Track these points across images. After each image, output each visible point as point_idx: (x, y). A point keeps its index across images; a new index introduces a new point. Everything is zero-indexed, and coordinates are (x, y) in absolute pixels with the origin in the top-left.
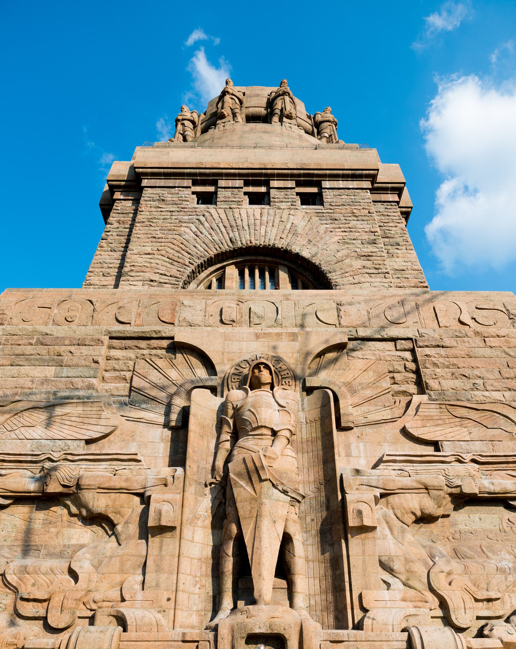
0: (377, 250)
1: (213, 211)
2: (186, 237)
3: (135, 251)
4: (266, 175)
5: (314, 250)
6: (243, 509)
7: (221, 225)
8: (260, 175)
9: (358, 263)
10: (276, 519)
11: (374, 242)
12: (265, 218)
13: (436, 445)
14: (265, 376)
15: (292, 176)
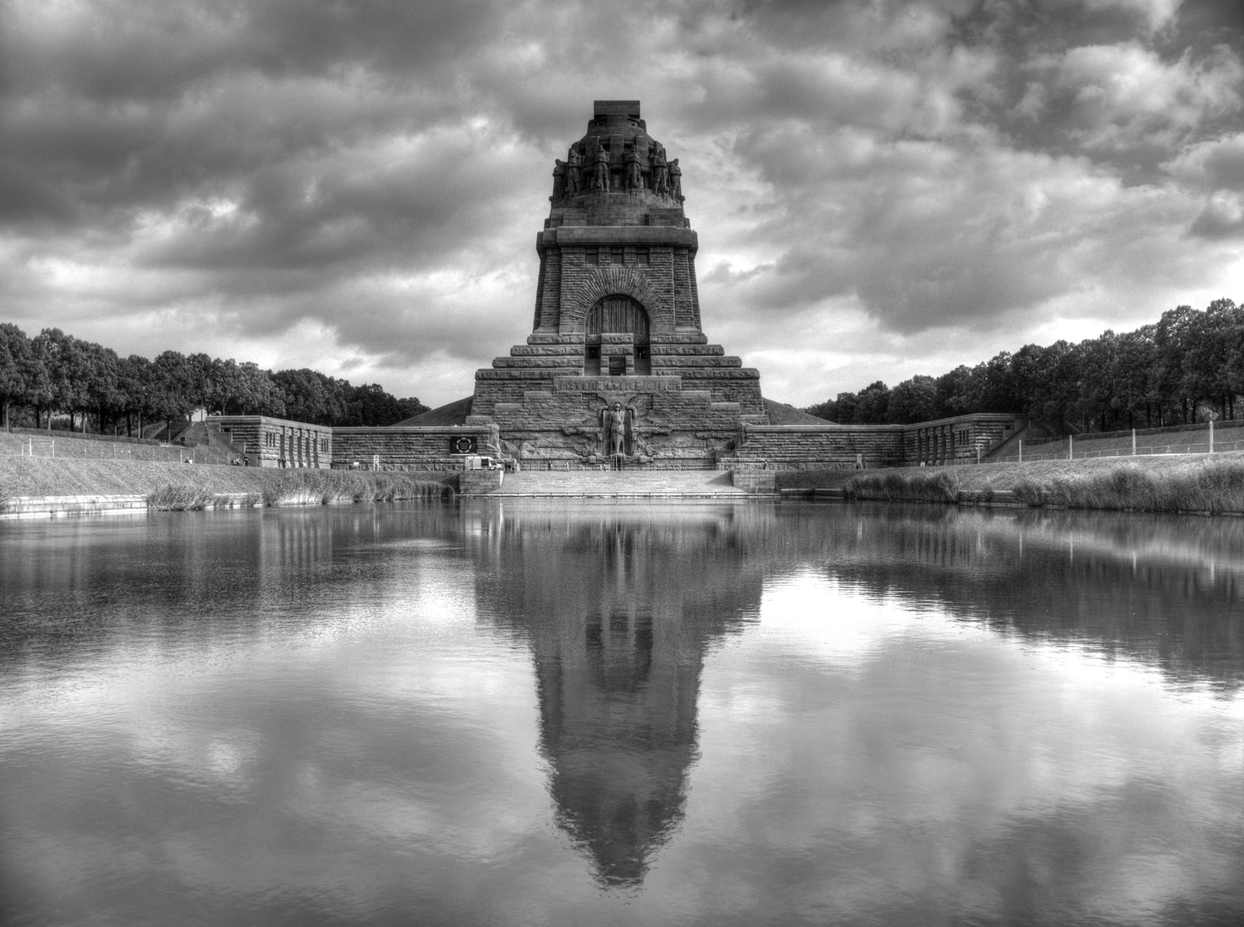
11: (669, 291)
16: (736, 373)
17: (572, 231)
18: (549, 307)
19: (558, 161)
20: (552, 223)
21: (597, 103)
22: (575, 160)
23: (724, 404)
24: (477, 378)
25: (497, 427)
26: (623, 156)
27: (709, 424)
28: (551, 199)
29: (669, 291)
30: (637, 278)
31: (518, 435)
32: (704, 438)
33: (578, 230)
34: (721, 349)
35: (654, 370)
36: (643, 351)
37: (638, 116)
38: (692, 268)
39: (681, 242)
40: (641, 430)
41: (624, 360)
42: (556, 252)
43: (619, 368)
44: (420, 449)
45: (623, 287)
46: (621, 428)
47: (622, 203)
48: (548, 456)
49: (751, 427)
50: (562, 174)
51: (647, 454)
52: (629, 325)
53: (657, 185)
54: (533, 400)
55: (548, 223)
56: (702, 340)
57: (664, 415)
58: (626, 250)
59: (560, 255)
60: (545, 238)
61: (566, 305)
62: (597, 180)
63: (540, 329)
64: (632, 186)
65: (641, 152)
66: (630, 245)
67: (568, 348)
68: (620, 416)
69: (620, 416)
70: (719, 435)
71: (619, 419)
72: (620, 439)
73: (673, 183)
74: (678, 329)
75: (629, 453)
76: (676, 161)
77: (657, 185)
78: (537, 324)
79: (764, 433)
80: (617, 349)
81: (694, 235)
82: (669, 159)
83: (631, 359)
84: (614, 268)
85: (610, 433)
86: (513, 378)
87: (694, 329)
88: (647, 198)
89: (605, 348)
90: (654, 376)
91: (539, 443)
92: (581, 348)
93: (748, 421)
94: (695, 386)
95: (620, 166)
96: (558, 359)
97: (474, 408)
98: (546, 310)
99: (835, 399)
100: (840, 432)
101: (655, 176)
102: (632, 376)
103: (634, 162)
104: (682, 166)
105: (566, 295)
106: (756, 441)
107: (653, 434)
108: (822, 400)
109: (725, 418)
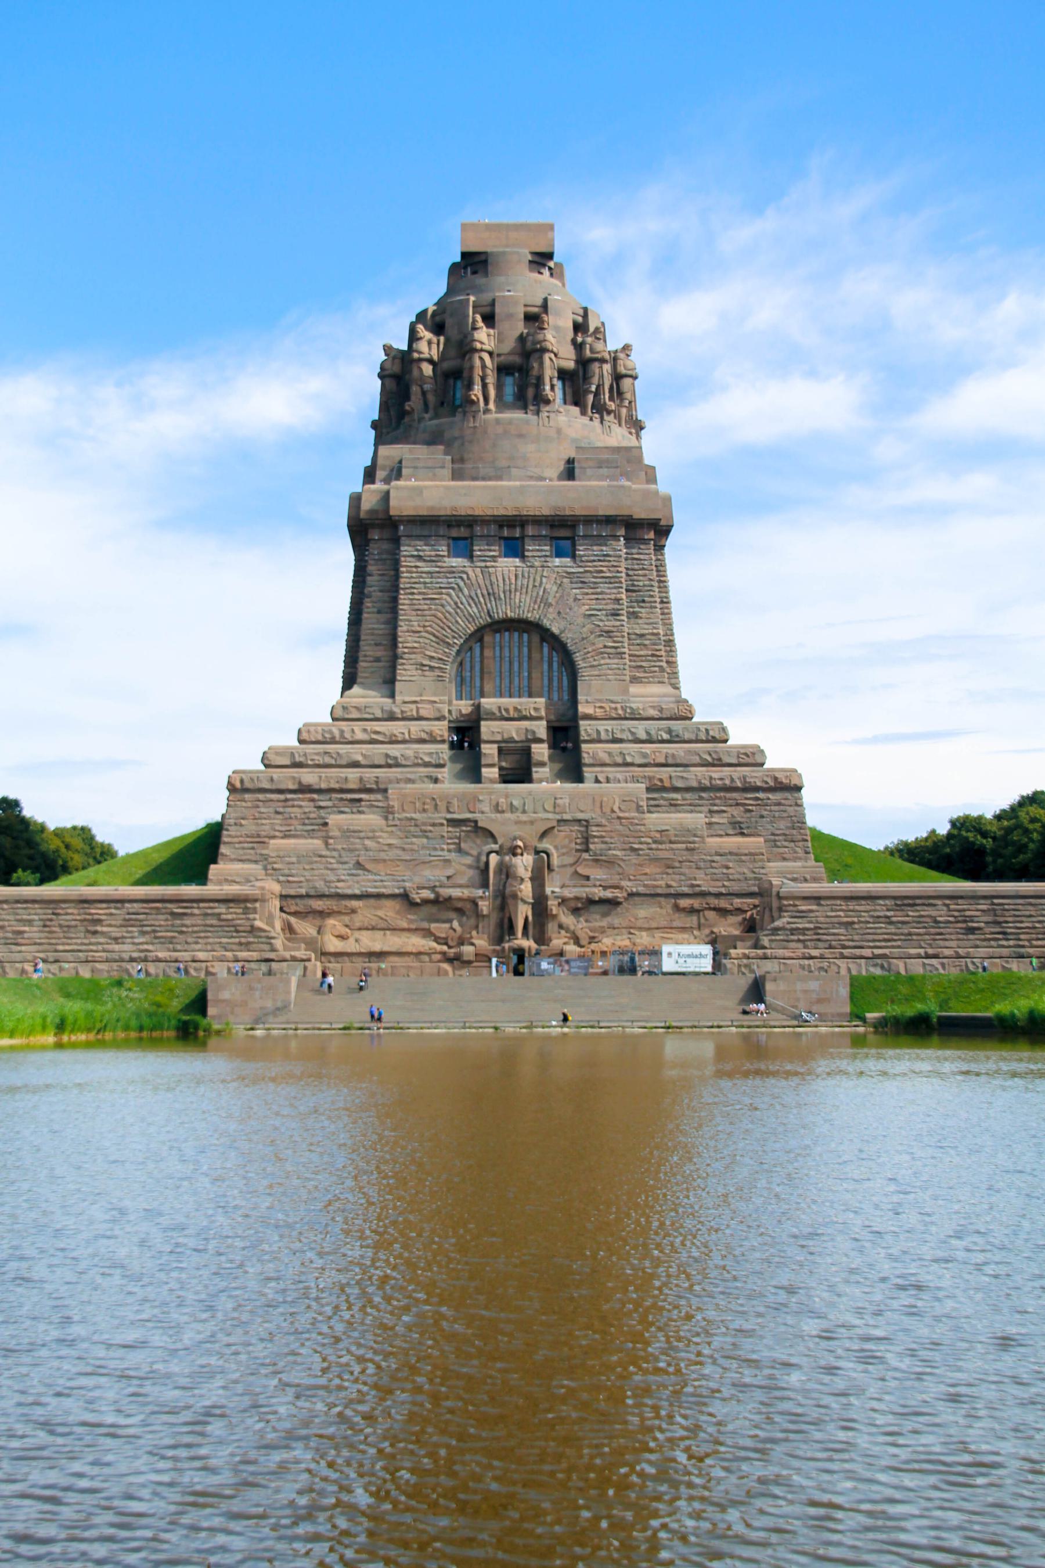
0: (618, 623)
1: (471, 573)
2: (448, 608)
3: (405, 628)
4: (521, 521)
5: (563, 624)
6: (512, 908)
7: (479, 591)
8: (515, 521)
9: (600, 642)
10: (523, 912)
11: (615, 614)
12: (519, 583)
13: (588, 878)
14: (519, 851)
15: (547, 521)
16: (754, 776)
17: (419, 491)
18: (371, 649)
19: (387, 349)
20: (380, 474)
22: (423, 346)
23: (735, 842)
24: (232, 788)
25: (277, 888)
26: (522, 339)
27: (704, 883)
28: (375, 425)
29: (615, 614)
30: (552, 588)
31: (318, 904)
32: (692, 911)
33: (427, 486)
34: (724, 730)
35: (588, 773)
36: (565, 735)
37: (550, 256)
38: (660, 568)
39: (640, 513)
40: (568, 893)
41: (527, 752)
42: (386, 534)
43: (519, 771)
44: (115, 932)
45: (523, 607)
46: (526, 889)
47: (521, 436)
48: (377, 947)
49: (791, 887)
50: (397, 373)
51: (577, 942)
52: (536, 684)
53: (590, 398)
54: (348, 833)
55: (370, 475)
57: (610, 863)
58: (530, 531)
59: (396, 541)
60: (366, 505)
61: (406, 639)
62: (469, 386)
63: (356, 690)
64: (541, 400)
65: (557, 329)
66: (538, 521)
67: (416, 728)
70: (723, 903)
72: (523, 912)
73: (620, 394)
74: (634, 689)
75: (541, 939)
77: (590, 398)
78: (349, 680)
79: (817, 899)
80: (514, 730)
81: (667, 500)
82: (613, 344)
83: (541, 751)
84: (508, 565)
85: (504, 901)
86: (304, 789)
87: (668, 689)
88: (567, 425)
89: (487, 728)
90: (588, 786)
92: (441, 729)
93: (782, 874)
94: (673, 805)
95: (517, 359)
96: (395, 750)
97: (223, 849)
98: (367, 650)
99: (943, 829)
100: (975, 897)
101: (586, 378)
102: (546, 785)
103: (544, 350)
104: (637, 360)
105: (408, 622)
106: (802, 915)
107: (591, 902)
108: (914, 833)
109: (736, 869)
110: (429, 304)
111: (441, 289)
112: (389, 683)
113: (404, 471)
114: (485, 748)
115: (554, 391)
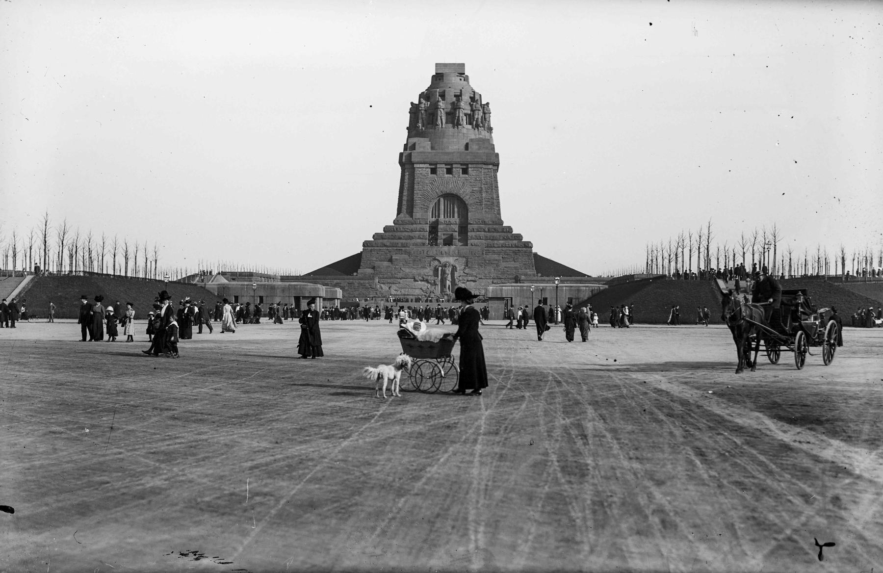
19: (412, 103)
21: (437, 64)
24: (364, 245)
26: (453, 103)
36: (463, 229)
43: (448, 242)
56: (502, 222)
62: (437, 120)
64: (458, 124)
68: (448, 271)
69: (448, 271)
71: (447, 272)
76: (488, 103)
78: (399, 211)
81: (497, 154)
82: (484, 102)
83: (456, 234)
89: (440, 226)
91: (400, 286)
110: (424, 90)
111: (429, 84)
112: (411, 212)
113: (417, 147)
114: (439, 234)
115: (464, 120)
